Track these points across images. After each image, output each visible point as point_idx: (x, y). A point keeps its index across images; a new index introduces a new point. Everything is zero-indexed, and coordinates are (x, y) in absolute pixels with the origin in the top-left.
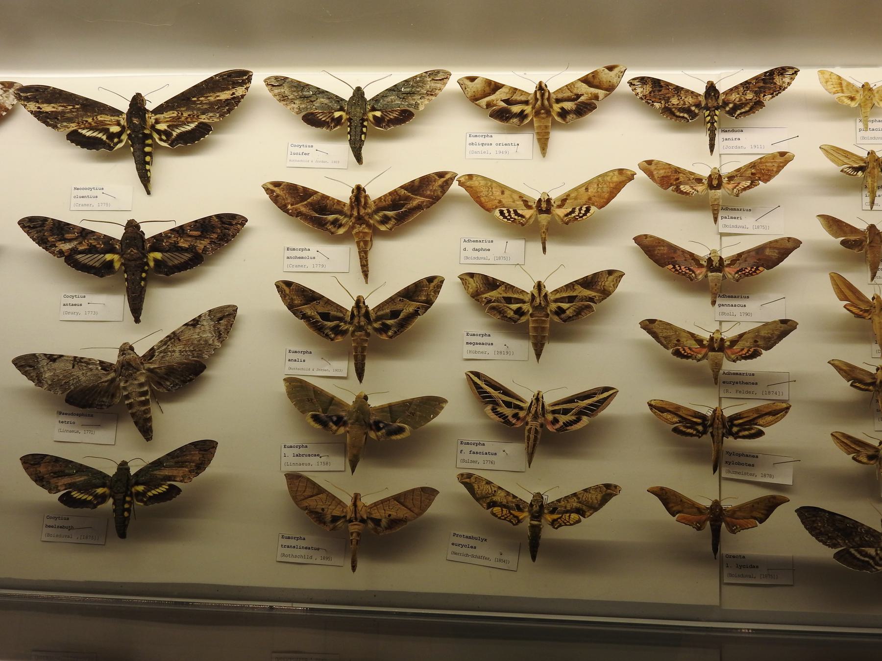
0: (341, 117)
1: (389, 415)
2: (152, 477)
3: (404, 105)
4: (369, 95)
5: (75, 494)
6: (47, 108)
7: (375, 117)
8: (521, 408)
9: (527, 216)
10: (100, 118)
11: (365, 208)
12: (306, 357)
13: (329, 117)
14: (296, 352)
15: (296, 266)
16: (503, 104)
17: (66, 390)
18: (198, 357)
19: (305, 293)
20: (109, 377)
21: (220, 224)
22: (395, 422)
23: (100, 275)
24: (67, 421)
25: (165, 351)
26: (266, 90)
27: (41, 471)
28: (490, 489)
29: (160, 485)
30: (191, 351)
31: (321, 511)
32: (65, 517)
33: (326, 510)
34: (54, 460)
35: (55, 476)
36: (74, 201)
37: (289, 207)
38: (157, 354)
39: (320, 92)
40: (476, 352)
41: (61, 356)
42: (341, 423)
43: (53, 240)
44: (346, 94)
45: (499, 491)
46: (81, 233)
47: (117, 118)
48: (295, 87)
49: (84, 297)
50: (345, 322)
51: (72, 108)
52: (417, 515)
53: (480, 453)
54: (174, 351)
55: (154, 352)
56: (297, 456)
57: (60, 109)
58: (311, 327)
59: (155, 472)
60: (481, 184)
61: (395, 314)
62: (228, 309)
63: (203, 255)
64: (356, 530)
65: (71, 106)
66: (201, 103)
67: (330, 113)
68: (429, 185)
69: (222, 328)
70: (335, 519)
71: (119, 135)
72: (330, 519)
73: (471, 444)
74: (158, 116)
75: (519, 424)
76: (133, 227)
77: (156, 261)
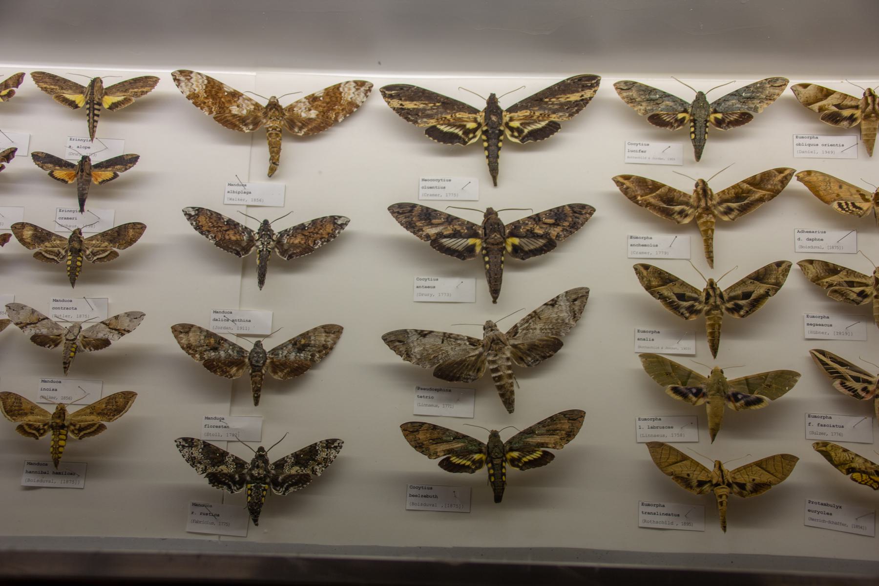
0: (684, 118)
1: (746, 387)
2: (525, 444)
3: (744, 109)
4: (711, 99)
5: (454, 460)
6: (409, 105)
7: (716, 119)
8: (870, 383)
9: (865, 208)
10: (458, 115)
11: (711, 200)
12: (654, 336)
13: (673, 118)
14: (644, 332)
15: (640, 253)
16: (835, 109)
17: (434, 364)
18: (556, 334)
19: (662, 276)
20: (477, 352)
21: (572, 213)
22: (753, 394)
23: (463, 258)
24: (425, 395)
25: (527, 329)
26: (615, 95)
27: (420, 438)
28: (847, 456)
29: (534, 451)
30: (549, 329)
31: (686, 477)
32: (428, 486)
33: (691, 475)
34: (432, 428)
35: (434, 442)
36: (422, 191)
37: (639, 198)
38: (520, 331)
39: (666, 96)
40: (816, 333)
41: (431, 332)
42: (701, 395)
43: (421, 225)
44: (689, 98)
45: (857, 459)
46: (447, 218)
47: (474, 115)
48: (643, 91)
49: (437, 280)
50: (700, 303)
51: (433, 106)
52: (781, 479)
53: (828, 426)
54: (535, 329)
55: (517, 329)
56: (652, 428)
57: (422, 106)
58: (667, 307)
59: (528, 440)
60: (819, 180)
61: (746, 295)
62: (582, 291)
63: (556, 241)
64: (725, 493)
65: (432, 103)
66: (553, 104)
67: (674, 114)
68: (768, 180)
69: (576, 308)
70: (701, 484)
71: (474, 131)
72: (697, 484)
73: (818, 417)
74: (512, 114)
75: (869, 397)
76: (490, 214)
77: (514, 246)
